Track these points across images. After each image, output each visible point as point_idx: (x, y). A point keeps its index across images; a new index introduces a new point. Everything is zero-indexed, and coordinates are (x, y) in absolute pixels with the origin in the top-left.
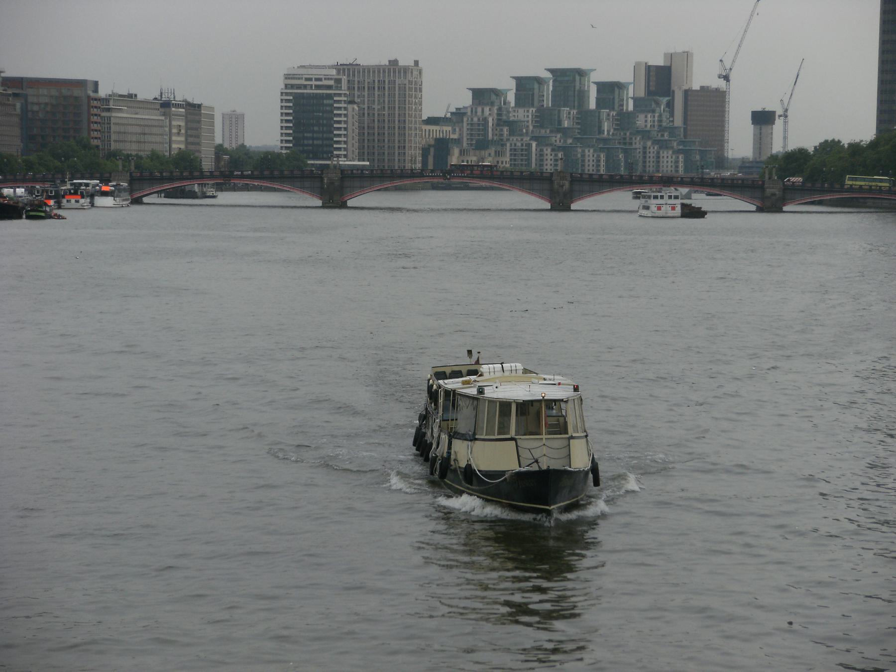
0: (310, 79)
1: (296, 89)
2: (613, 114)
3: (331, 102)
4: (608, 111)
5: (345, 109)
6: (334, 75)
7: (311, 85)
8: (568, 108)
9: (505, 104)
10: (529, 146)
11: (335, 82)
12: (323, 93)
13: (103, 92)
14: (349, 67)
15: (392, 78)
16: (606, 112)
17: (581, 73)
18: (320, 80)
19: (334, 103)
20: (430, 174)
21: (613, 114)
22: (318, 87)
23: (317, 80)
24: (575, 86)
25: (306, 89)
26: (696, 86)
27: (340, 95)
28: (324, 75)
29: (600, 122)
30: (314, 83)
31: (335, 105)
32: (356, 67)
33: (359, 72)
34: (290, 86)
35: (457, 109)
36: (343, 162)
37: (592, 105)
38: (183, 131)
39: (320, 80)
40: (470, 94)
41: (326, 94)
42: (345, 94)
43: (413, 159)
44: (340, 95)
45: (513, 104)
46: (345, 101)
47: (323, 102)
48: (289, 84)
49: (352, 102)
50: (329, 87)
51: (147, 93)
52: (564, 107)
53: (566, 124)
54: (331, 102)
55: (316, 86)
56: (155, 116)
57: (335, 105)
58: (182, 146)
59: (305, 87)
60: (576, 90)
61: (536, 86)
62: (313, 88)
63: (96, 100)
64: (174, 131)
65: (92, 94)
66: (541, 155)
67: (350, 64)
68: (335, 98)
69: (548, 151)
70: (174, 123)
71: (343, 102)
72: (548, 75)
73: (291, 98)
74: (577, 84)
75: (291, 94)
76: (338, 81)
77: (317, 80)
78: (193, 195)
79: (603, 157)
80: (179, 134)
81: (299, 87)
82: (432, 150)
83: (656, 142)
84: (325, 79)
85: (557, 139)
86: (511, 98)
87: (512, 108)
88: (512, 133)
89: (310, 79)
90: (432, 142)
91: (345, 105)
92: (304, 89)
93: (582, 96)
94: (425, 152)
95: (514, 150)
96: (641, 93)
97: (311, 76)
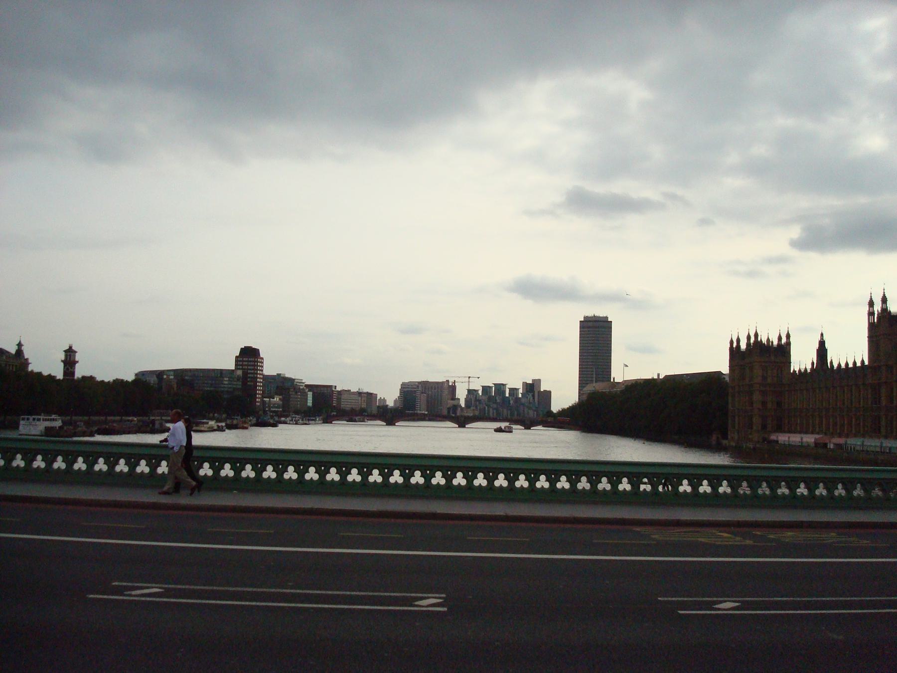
10: (485, 408)
13: (338, 389)
17: (504, 385)
22: (411, 388)
23: (412, 386)
26: (542, 390)
29: (509, 401)
36: (419, 412)
37: (507, 395)
38: (366, 401)
43: (445, 412)
45: (481, 394)
50: (415, 388)
51: (354, 389)
53: (498, 401)
56: (356, 397)
58: (365, 406)
63: (335, 391)
64: (363, 401)
65: (334, 389)
66: (489, 411)
69: (491, 410)
70: (363, 399)
72: (493, 385)
79: (509, 412)
80: (364, 402)
82: (452, 409)
83: (527, 407)
85: (495, 406)
86: (480, 393)
88: (480, 403)
90: (452, 406)
93: (504, 392)
94: (449, 409)
95: (480, 410)
96: (525, 392)
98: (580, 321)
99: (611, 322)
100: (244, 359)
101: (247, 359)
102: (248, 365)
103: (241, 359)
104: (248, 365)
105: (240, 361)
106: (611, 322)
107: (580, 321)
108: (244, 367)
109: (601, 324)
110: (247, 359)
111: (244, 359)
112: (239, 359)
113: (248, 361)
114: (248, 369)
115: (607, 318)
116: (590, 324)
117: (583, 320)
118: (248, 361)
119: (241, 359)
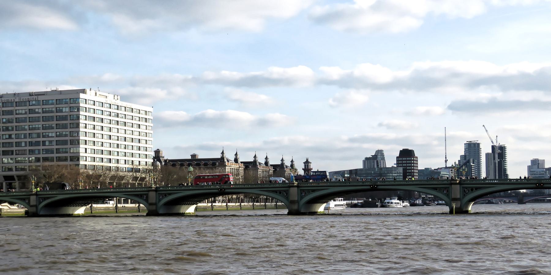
0: (537, 172)
18: (540, 172)
22: (540, 174)
23: (539, 172)
39: (540, 172)
50: (543, 174)
55: (539, 174)
59: (536, 174)
76: (546, 172)
77: (539, 172)
78: (493, 203)
81: (534, 174)
89: (537, 172)
100: (403, 159)
101: (405, 159)
102: (406, 163)
103: (401, 159)
104: (406, 163)
105: (400, 160)
108: (404, 165)
110: (405, 159)
111: (403, 159)
112: (399, 159)
113: (406, 160)
114: (406, 166)
118: (406, 160)
119: (401, 159)
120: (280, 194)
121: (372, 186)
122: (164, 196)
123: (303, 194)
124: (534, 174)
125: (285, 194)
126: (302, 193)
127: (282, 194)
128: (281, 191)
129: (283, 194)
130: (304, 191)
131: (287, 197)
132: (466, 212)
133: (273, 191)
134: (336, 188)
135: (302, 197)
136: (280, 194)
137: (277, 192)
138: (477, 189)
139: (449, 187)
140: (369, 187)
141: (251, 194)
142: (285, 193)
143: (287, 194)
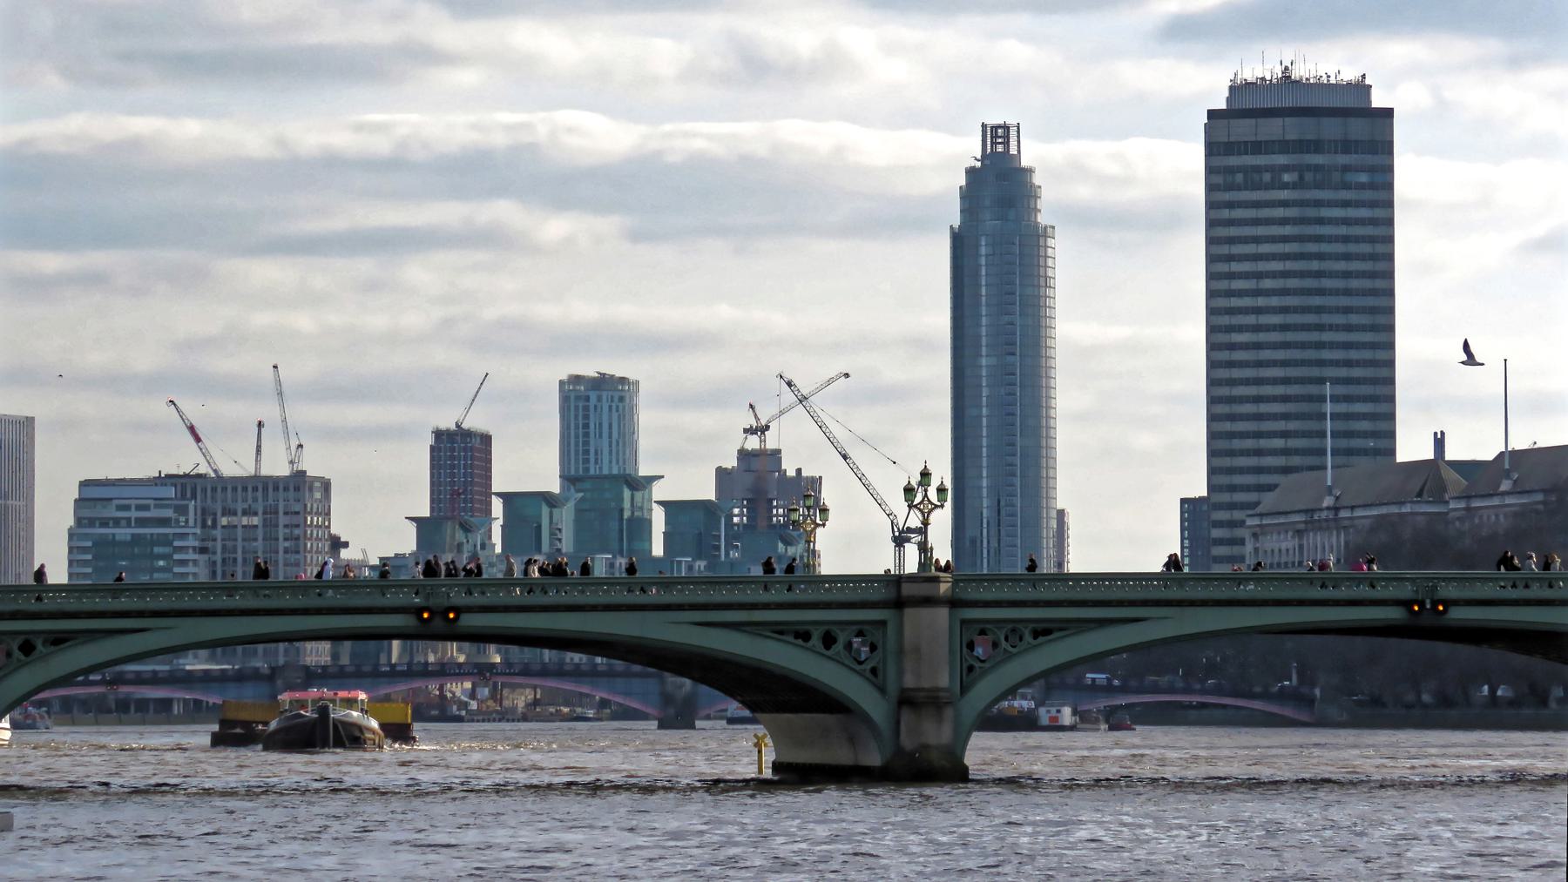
1: (100, 527)
2: (699, 567)
3: (167, 550)
4: (690, 559)
5: (195, 562)
6: (171, 499)
7: (129, 520)
8: (609, 553)
9: (483, 546)
11: (175, 512)
12: (152, 535)
14: (183, 481)
15: (271, 501)
16: (686, 561)
18: (146, 508)
19: (174, 552)
20: (457, 671)
21: (699, 567)
22: (142, 522)
23: (139, 508)
24: (622, 511)
25: (119, 527)
27: (183, 536)
28: (156, 499)
30: (134, 514)
31: (176, 557)
32: (198, 481)
33: (204, 490)
34: (86, 521)
35: (381, 559)
39: (146, 508)
40: (412, 529)
41: (158, 534)
42: (195, 534)
44: (183, 536)
45: (498, 549)
46: (194, 548)
47: (152, 550)
48: (84, 518)
49: (203, 550)
50: (164, 522)
52: (602, 553)
54: (167, 550)
55: (137, 520)
57: (176, 557)
59: (117, 522)
60: (625, 517)
61: (545, 510)
62: (133, 524)
67: (186, 476)
68: (176, 543)
71: (191, 551)
73: (89, 544)
74: (627, 505)
75: (86, 536)
76: (182, 510)
77: (139, 508)
81: (104, 523)
84: (156, 506)
87: (498, 556)
89: (127, 508)
91: (196, 557)
92: (114, 527)
93: (641, 527)
97: (127, 502)
98: (1212, 114)
99: (1388, 113)
106: (1388, 113)
107: (1212, 114)
109: (1331, 129)
115: (1361, 88)
116: (1272, 129)
117: (1222, 105)
120: (828, 647)
121: (1421, 604)
122: (17, 654)
123: (979, 651)
124: (104, 523)
125: (866, 649)
126: (971, 646)
127: (839, 647)
128: (835, 630)
129: (849, 645)
130: (983, 632)
131: (874, 671)
132: (957, 774)
133: (779, 631)
134: (1190, 611)
135: (971, 669)
136: (828, 647)
137: (805, 636)
138: (1043, 631)
139: (882, 624)
140: (1394, 614)
141: (282, 646)
142: (863, 644)
143: (873, 648)
